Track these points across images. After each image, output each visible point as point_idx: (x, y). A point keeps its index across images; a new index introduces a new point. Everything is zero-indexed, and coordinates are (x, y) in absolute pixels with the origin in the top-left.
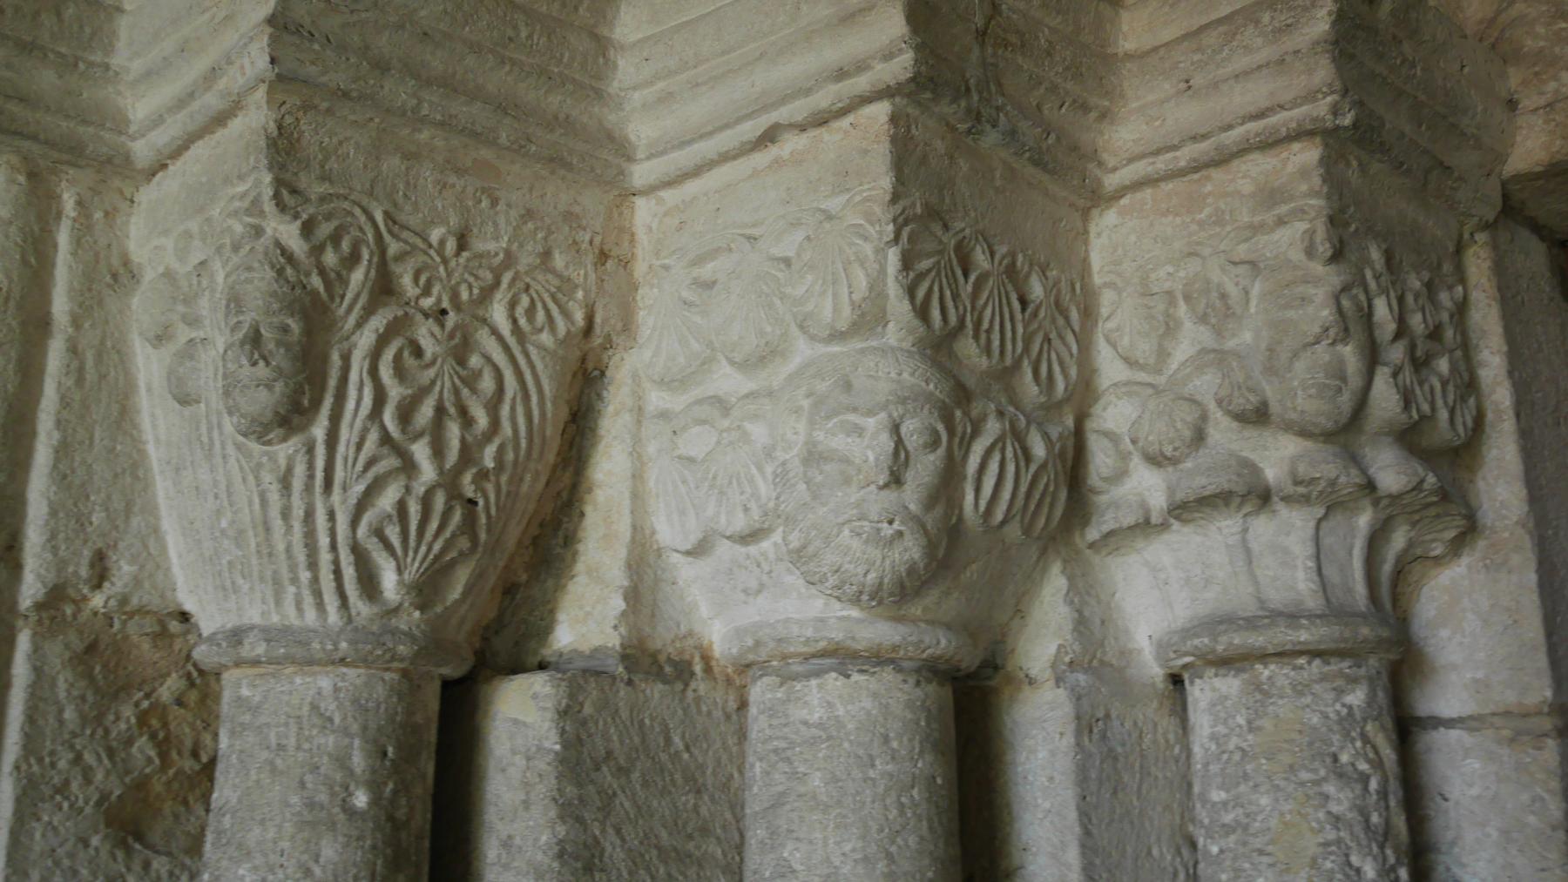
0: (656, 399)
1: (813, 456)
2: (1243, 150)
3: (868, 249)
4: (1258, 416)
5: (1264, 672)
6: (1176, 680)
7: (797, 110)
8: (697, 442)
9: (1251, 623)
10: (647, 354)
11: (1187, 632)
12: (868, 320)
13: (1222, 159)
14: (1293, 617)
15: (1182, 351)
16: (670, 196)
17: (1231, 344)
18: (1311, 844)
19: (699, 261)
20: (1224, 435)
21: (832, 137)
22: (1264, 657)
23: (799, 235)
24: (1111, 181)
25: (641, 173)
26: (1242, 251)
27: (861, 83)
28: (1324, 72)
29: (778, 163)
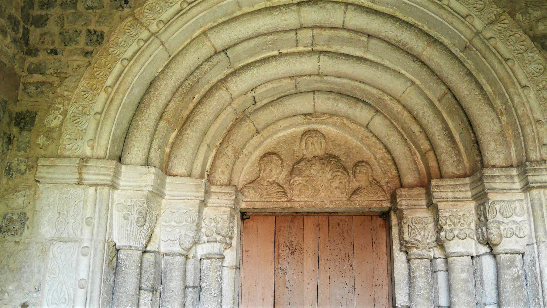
0: (164, 223)
1: (185, 235)
2: (224, 206)
3: (195, 215)
4: (219, 234)
5: (213, 260)
6: (201, 259)
7: (189, 198)
8: (169, 229)
9: (213, 254)
11: (206, 255)
12: (193, 222)
13: (221, 207)
14: (217, 254)
15: (212, 225)
16: (169, 201)
17: (218, 226)
18: (215, 277)
20: (215, 235)
21: (192, 202)
22: (213, 258)
23: (186, 211)
24: (208, 205)
25: (166, 197)
26: (220, 217)
27: (198, 198)
28: (233, 202)
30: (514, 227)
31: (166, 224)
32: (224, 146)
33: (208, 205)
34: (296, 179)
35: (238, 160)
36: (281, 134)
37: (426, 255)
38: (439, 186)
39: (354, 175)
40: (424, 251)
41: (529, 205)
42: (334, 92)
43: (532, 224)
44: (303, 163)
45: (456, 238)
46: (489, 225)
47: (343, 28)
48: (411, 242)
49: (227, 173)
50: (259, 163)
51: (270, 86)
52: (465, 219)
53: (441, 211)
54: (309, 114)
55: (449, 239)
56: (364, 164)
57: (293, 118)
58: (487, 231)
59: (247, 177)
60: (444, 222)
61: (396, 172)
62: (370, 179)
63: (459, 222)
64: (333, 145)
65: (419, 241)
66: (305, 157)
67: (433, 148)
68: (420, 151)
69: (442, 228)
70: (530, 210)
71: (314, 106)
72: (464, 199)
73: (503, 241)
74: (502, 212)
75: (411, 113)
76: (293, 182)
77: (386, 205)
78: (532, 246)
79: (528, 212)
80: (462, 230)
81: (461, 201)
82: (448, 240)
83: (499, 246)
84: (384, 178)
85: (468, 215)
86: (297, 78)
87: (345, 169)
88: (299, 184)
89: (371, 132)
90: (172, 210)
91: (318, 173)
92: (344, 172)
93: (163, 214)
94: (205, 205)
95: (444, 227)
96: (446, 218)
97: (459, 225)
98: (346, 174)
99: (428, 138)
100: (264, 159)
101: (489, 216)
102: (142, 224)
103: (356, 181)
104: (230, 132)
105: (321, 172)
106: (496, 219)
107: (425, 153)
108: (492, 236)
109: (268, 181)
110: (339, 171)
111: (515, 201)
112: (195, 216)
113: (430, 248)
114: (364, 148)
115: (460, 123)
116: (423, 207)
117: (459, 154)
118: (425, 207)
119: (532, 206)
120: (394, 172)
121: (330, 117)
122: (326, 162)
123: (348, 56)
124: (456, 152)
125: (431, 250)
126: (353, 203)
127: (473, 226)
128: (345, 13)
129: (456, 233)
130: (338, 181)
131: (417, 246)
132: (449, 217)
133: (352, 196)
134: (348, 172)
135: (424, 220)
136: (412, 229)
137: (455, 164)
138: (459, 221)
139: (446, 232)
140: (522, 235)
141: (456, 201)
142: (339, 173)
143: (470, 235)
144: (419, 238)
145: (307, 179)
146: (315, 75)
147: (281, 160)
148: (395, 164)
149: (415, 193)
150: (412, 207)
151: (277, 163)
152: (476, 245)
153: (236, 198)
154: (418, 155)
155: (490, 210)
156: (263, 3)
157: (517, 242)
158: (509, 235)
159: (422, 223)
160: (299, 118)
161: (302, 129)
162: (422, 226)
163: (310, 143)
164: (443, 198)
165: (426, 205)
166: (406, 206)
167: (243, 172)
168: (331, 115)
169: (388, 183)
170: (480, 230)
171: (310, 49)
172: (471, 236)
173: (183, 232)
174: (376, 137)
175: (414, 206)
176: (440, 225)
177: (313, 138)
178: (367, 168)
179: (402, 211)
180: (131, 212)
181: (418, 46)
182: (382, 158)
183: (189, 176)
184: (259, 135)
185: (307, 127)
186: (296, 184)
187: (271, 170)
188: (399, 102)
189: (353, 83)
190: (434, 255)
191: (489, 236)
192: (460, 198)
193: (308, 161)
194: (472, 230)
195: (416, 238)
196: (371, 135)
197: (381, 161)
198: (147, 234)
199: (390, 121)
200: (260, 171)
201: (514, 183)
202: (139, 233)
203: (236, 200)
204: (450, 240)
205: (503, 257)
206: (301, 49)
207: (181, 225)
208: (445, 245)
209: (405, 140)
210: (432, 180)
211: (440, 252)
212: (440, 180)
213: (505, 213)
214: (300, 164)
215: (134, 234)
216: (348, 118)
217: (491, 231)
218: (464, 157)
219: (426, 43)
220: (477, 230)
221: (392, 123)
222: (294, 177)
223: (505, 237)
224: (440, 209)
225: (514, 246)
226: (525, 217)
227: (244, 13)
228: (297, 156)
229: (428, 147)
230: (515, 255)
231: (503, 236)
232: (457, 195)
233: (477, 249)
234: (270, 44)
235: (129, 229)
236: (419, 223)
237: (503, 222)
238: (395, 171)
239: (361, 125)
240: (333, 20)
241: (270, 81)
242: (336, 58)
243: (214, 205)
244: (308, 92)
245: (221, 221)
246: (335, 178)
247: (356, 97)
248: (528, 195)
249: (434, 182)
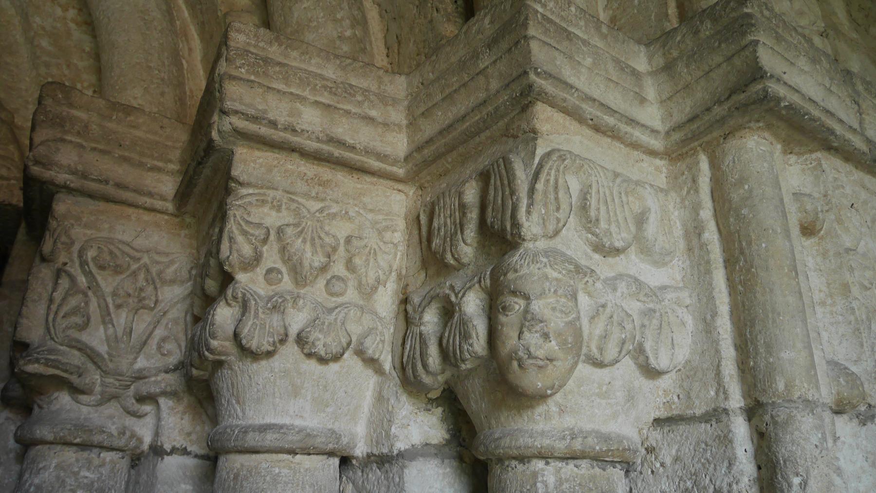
30: (634, 307)
37: (113, 429)
38: (266, 61)
40: (112, 409)
41: (707, 213)
45: (291, 350)
48: (51, 351)
52: (357, 261)
53: (244, 191)
55: (254, 344)
60: (247, 250)
63: (324, 269)
65: (92, 355)
69: (227, 279)
70: (711, 234)
72: (375, 164)
73: (571, 385)
74: (593, 213)
80: (330, 311)
83: (540, 409)
95: (241, 277)
97: (321, 283)
101: (535, 216)
106: (557, 243)
108: (532, 338)
113: (141, 399)
118: (170, 207)
125: (147, 408)
129: (297, 320)
131: (74, 379)
132: (280, 231)
138: (324, 260)
140: (662, 361)
143: (368, 342)
149: (138, 133)
152: (380, 398)
155: (540, 186)
157: (631, 397)
158: (611, 352)
159: (134, 274)
164: (273, 124)
166: (74, 172)
175: (118, 185)
190: (157, 434)
191: (510, 340)
192: (352, 148)
194: (380, 319)
195: (84, 337)
201: (643, 100)
205: (551, 480)
208: (224, 381)
211: (186, 422)
213: (603, 225)
217: (537, 306)
224: (243, 178)
225: (615, 416)
230: (610, 470)
231: (584, 350)
232: (342, 129)
236: (118, 270)
248: (704, 165)
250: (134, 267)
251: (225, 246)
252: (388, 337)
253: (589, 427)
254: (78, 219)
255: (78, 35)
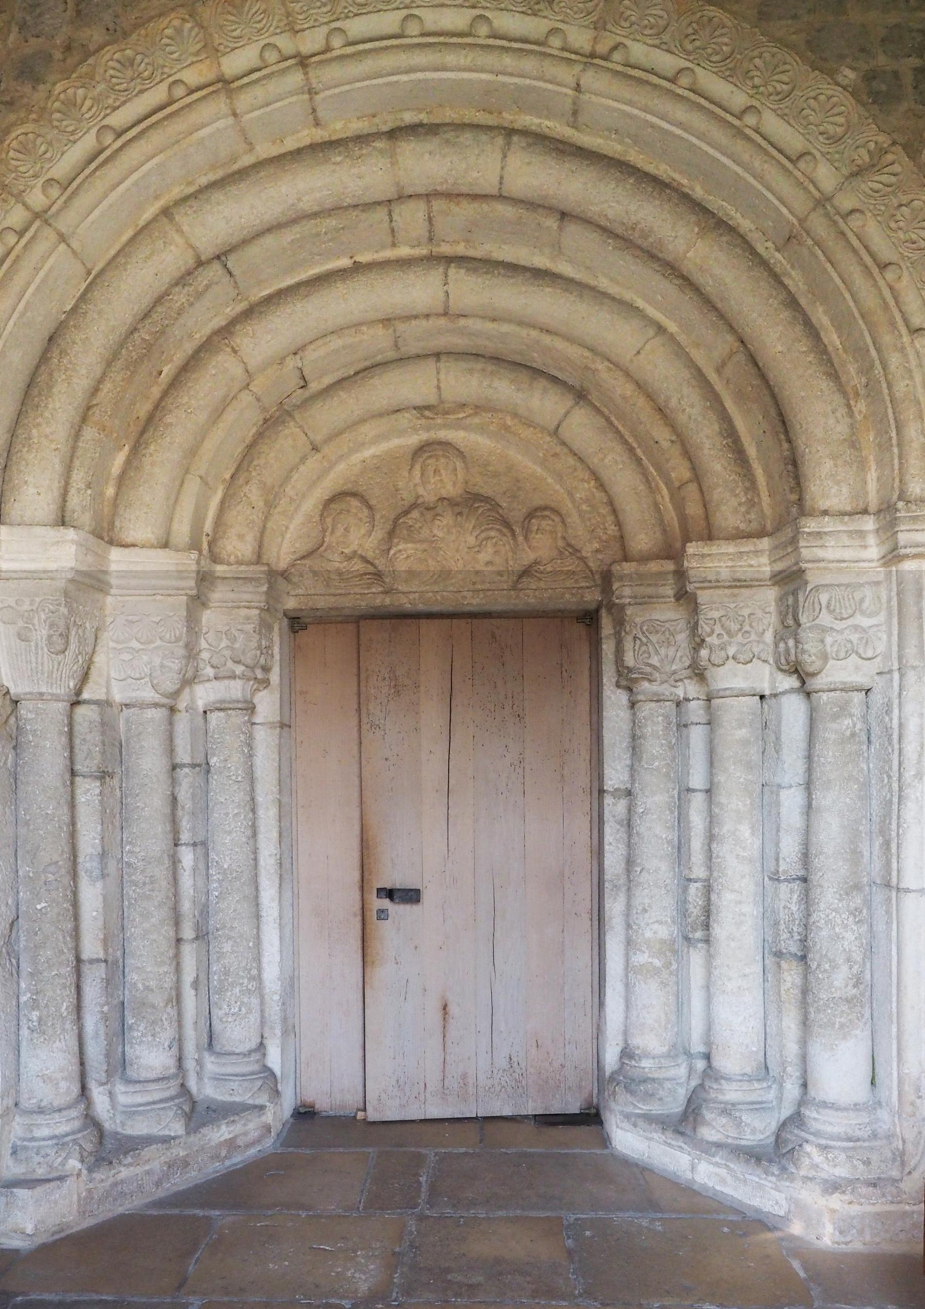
0: (112, 644)
7: (166, 592)
8: (126, 657)
10: (111, 634)
12: (178, 640)
13: (239, 607)
19: (128, 615)
21: (170, 599)
24: (211, 605)
25: (113, 591)
27: (182, 592)
29: (155, 600)
31: (120, 646)
32: (241, 481)
33: (211, 605)
34: (400, 547)
35: (276, 511)
36: (368, 453)
39: (526, 538)
42: (483, 356)
43: (895, 632)
44: (415, 514)
45: (731, 661)
46: (802, 634)
47: (501, 197)
49: (250, 538)
50: (322, 515)
51: (336, 343)
54: (428, 407)
56: (547, 513)
57: (394, 417)
58: (797, 647)
59: (297, 545)
60: (708, 629)
61: (617, 528)
62: (561, 543)
63: (740, 630)
64: (481, 473)
66: (420, 501)
67: (697, 476)
68: (668, 483)
69: (703, 641)
71: (439, 388)
73: (828, 666)
75: (652, 400)
76: (395, 554)
77: (592, 597)
78: (888, 676)
79: (889, 608)
81: (747, 587)
82: (714, 665)
83: (819, 676)
84: (590, 541)
85: (759, 614)
86: (397, 323)
87: (507, 524)
88: (408, 557)
89: (564, 443)
90: (130, 618)
91: (449, 532)
92: (505, 530)
93: (112, 626)
94: (204, 605)
95: (707, 639)
96: (712, 622)
98: (509, 535)
99: (687, 454)
100: (332, 506)
102: (60, 647)
103: (529, 547)
104: (252, 448)
105: (454, 530)
107: (679, 488)
109: (342, 553)
110: (491, 529)
111: (862, 585)
112: (180, 629)
114: (550, 480)
115: (761, 417)
116: (668, 600)
117: (752, 485)
118: (673, 600)
119: (898, 594)
120: (612, 530)
121: (476, 414)
122: (466, 511)
123: (513, 268)
124: (747, 484)
126: (521, 594)
127: (769, 637)
128: (505, 156)
129: (731, 651)
130: (490, 550)
133: (521, 581)
134: (513, 532)
135: (667, 625)
136: (642, 644)
137: (743, 509)
139: (711, 649)
140: (870, 654)
141: (736, 587)
142: (492, 533)
144: (655, 661)
145: (425, 546)
146: (438, 315)
147: (370, 507)
148: (614, 512)
150: (644, 601)
151: (360, 515)
152: (771, 674)
153: (271, 588)
154: (665, 491)
156: (306, 132)
157: (857, 668)
160: (407, 415)
161: (414, 440)
162: (663, 638)
163: (431, 469)
165: (675, 596)
166: (631, 597)
167: (288, 536)
168: (478, 408)
169: (598, 551)
170: (782, 645)
171: (424, 252)
172: (763, 656)
173: (157, 661)
174: (575, 454)
175: (649, 597)
176: (699, 636)
177: (437, 460)
178: (553, 521)
179: (622, 607)
180: (33, 625)
181: (676, 237)
182: (587, 500)
183: (165, 545)
184: (318, 456)
185: (424, 436)
186: (402, 557)
187: (347, 530)
188: (627, 374)
189: (524, 332)
193: (428, 509)
196: (566, 450)
197: (584, 507)
198: (75, 668)
199: (607, 419)
200: (324, 531)
202: (56, 666)
203: (272, 594)
204: (719, 666)
206: (404, 251)
207: (153, 646)
209: (639, 461)
210: (688, 544)
212: (706, 544)
214: (409, 516)
215: (46, 669)
216: (515, 415)
218: (762, 494)
219: (696, 230)
220: (776, 645)
221: (611, 423)
222: (398, 544)
223: (834, 659)
226: (881, 618)
227: (260, 159)
228: (403, 500)
229: (687, 475)
230: (850, 693)
233: (773, 682)
234: (330, 240)
235: (33, 659)
237: (832, 628)
238: (613, 527)
239: (543, 429)
240: (475, 174)
241: (337, 331)
242: (487, 273)
243: (225, 604)
244: (426, 356)
245: (241, 637)
246: (484, 543)
247: (534, 365)
249: (691, 548)
250: (663, 629)
251: (700, 629)
252: (770, 651)
253: (838, 680)
254: (636, 615)
255: (599, 495)
